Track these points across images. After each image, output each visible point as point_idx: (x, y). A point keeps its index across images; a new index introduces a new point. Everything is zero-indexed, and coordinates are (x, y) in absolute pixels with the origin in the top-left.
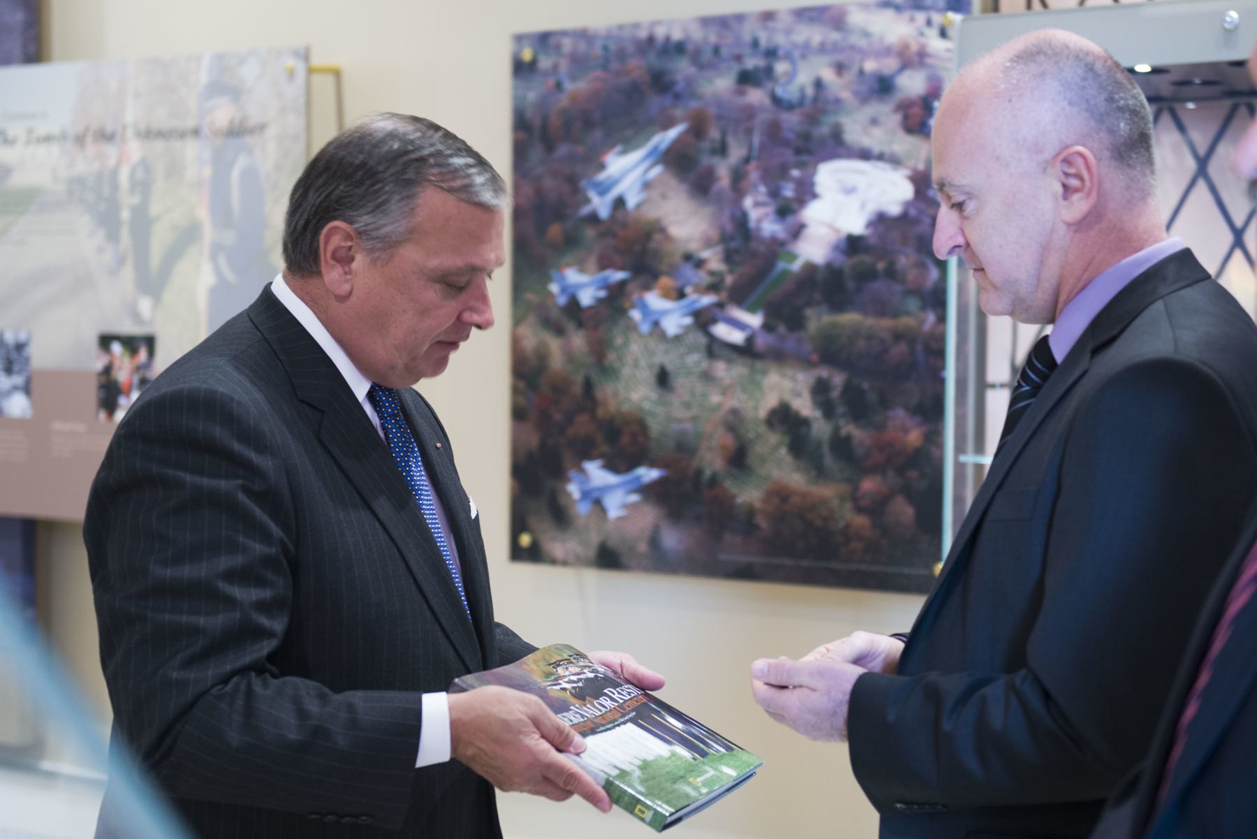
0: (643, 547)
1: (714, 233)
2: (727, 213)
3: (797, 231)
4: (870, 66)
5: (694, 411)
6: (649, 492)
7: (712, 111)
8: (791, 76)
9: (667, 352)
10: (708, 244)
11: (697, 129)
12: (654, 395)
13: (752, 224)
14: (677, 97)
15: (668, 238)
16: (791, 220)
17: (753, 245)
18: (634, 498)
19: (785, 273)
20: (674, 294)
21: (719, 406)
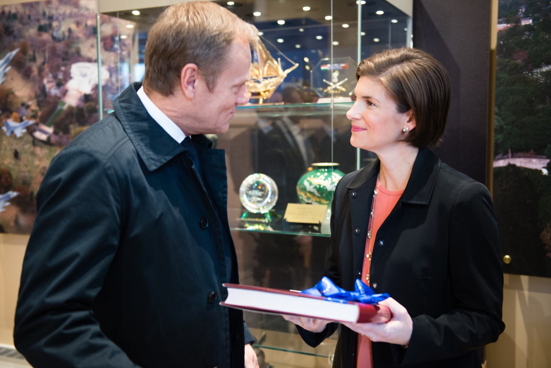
0: (12, 224)
1: (33, 94)
2: (37, 86)
3: (65, 93)
4: (90, 23)
5: (29, 168)
6: (13, 201)
7: (29, 43)
8: (59, 27)
9: (17, 144)
10: (30, 99)
11: (24, 51)
12: (13, 162)
13: (47, 90)
14: (15, 37)
15: (15, 96)
16: (62, 88)
17: (48, 99)
18: (8, 204)
19: (61, 110)
20: (19, 120)
21: (38, 166)
